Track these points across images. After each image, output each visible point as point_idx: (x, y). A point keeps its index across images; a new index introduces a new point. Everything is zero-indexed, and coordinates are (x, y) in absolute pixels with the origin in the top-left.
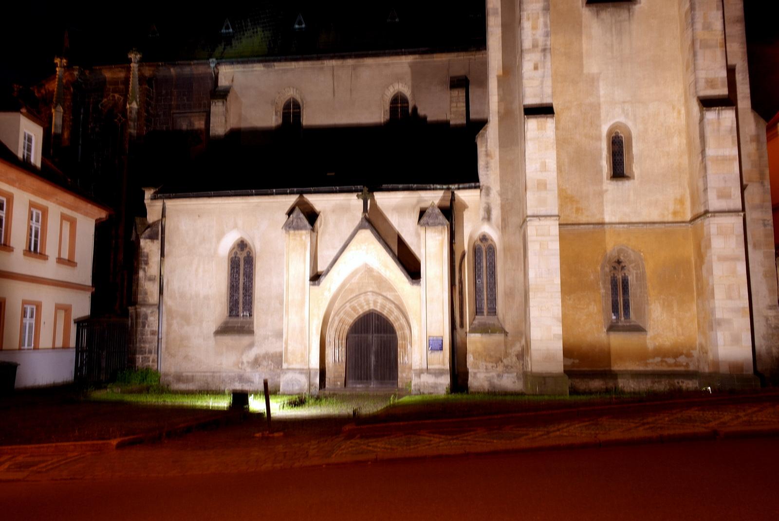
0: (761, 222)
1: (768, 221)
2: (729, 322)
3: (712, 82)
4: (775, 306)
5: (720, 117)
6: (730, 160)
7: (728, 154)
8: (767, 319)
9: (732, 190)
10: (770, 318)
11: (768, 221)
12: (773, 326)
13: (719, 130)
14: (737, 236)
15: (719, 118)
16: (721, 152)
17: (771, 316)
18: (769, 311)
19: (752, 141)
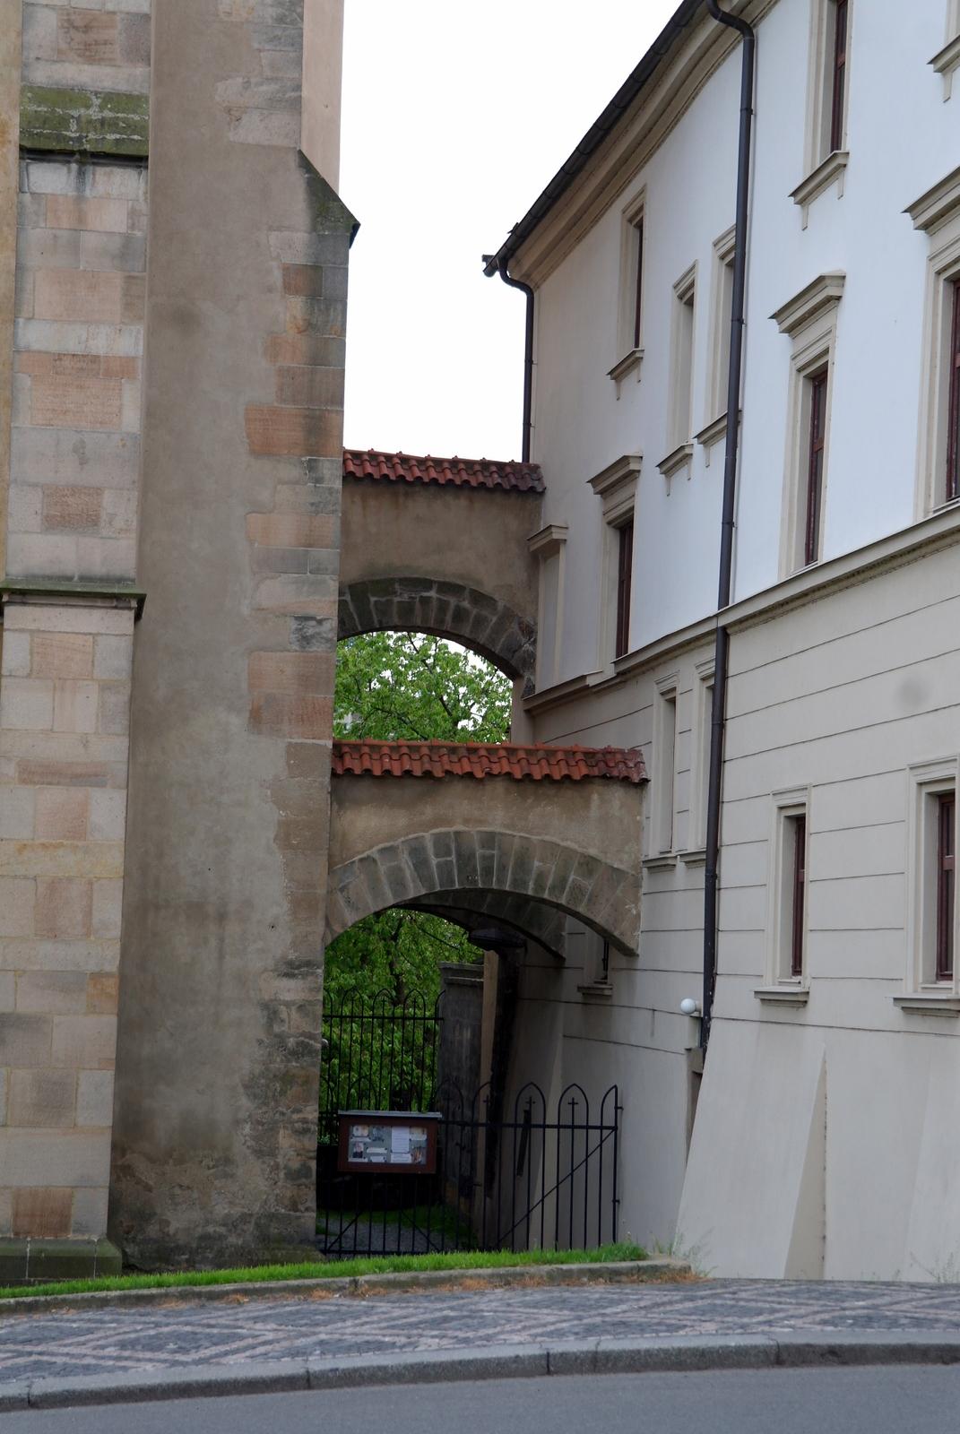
0: (294, 625)
1: (320, 622)
2: (31, 1024)
3: (87, 29)
4: (308, 964)
5: (88, 193)
6: (109, 374)
7: (102, 352)
8: (271, 1011)
9: (108, 498)
10: (284, 1015)
11: (320, 622)
12: (291, 1042)
13: (75, 248)
14: (105, 687)
15: (80, 199)
16: (73, 339)
17: (288, 1004)
18: (291, 983)
19: (289, 288)
